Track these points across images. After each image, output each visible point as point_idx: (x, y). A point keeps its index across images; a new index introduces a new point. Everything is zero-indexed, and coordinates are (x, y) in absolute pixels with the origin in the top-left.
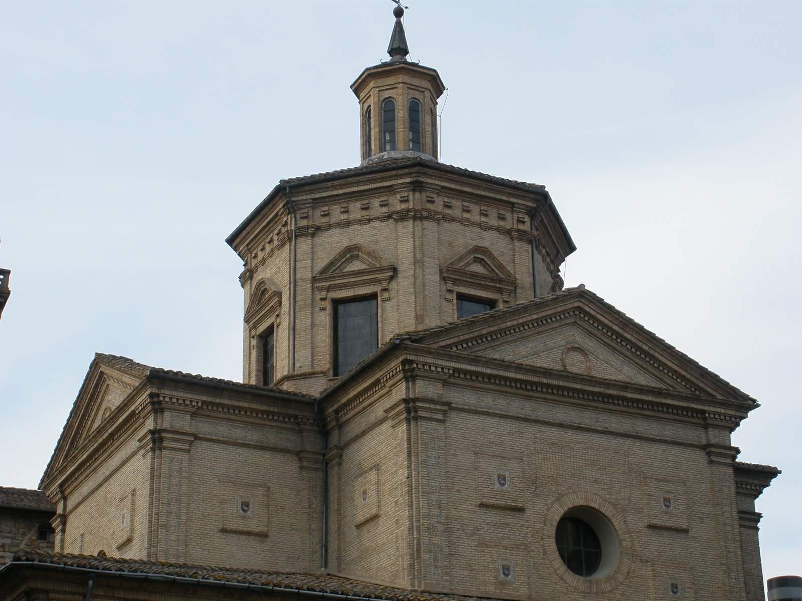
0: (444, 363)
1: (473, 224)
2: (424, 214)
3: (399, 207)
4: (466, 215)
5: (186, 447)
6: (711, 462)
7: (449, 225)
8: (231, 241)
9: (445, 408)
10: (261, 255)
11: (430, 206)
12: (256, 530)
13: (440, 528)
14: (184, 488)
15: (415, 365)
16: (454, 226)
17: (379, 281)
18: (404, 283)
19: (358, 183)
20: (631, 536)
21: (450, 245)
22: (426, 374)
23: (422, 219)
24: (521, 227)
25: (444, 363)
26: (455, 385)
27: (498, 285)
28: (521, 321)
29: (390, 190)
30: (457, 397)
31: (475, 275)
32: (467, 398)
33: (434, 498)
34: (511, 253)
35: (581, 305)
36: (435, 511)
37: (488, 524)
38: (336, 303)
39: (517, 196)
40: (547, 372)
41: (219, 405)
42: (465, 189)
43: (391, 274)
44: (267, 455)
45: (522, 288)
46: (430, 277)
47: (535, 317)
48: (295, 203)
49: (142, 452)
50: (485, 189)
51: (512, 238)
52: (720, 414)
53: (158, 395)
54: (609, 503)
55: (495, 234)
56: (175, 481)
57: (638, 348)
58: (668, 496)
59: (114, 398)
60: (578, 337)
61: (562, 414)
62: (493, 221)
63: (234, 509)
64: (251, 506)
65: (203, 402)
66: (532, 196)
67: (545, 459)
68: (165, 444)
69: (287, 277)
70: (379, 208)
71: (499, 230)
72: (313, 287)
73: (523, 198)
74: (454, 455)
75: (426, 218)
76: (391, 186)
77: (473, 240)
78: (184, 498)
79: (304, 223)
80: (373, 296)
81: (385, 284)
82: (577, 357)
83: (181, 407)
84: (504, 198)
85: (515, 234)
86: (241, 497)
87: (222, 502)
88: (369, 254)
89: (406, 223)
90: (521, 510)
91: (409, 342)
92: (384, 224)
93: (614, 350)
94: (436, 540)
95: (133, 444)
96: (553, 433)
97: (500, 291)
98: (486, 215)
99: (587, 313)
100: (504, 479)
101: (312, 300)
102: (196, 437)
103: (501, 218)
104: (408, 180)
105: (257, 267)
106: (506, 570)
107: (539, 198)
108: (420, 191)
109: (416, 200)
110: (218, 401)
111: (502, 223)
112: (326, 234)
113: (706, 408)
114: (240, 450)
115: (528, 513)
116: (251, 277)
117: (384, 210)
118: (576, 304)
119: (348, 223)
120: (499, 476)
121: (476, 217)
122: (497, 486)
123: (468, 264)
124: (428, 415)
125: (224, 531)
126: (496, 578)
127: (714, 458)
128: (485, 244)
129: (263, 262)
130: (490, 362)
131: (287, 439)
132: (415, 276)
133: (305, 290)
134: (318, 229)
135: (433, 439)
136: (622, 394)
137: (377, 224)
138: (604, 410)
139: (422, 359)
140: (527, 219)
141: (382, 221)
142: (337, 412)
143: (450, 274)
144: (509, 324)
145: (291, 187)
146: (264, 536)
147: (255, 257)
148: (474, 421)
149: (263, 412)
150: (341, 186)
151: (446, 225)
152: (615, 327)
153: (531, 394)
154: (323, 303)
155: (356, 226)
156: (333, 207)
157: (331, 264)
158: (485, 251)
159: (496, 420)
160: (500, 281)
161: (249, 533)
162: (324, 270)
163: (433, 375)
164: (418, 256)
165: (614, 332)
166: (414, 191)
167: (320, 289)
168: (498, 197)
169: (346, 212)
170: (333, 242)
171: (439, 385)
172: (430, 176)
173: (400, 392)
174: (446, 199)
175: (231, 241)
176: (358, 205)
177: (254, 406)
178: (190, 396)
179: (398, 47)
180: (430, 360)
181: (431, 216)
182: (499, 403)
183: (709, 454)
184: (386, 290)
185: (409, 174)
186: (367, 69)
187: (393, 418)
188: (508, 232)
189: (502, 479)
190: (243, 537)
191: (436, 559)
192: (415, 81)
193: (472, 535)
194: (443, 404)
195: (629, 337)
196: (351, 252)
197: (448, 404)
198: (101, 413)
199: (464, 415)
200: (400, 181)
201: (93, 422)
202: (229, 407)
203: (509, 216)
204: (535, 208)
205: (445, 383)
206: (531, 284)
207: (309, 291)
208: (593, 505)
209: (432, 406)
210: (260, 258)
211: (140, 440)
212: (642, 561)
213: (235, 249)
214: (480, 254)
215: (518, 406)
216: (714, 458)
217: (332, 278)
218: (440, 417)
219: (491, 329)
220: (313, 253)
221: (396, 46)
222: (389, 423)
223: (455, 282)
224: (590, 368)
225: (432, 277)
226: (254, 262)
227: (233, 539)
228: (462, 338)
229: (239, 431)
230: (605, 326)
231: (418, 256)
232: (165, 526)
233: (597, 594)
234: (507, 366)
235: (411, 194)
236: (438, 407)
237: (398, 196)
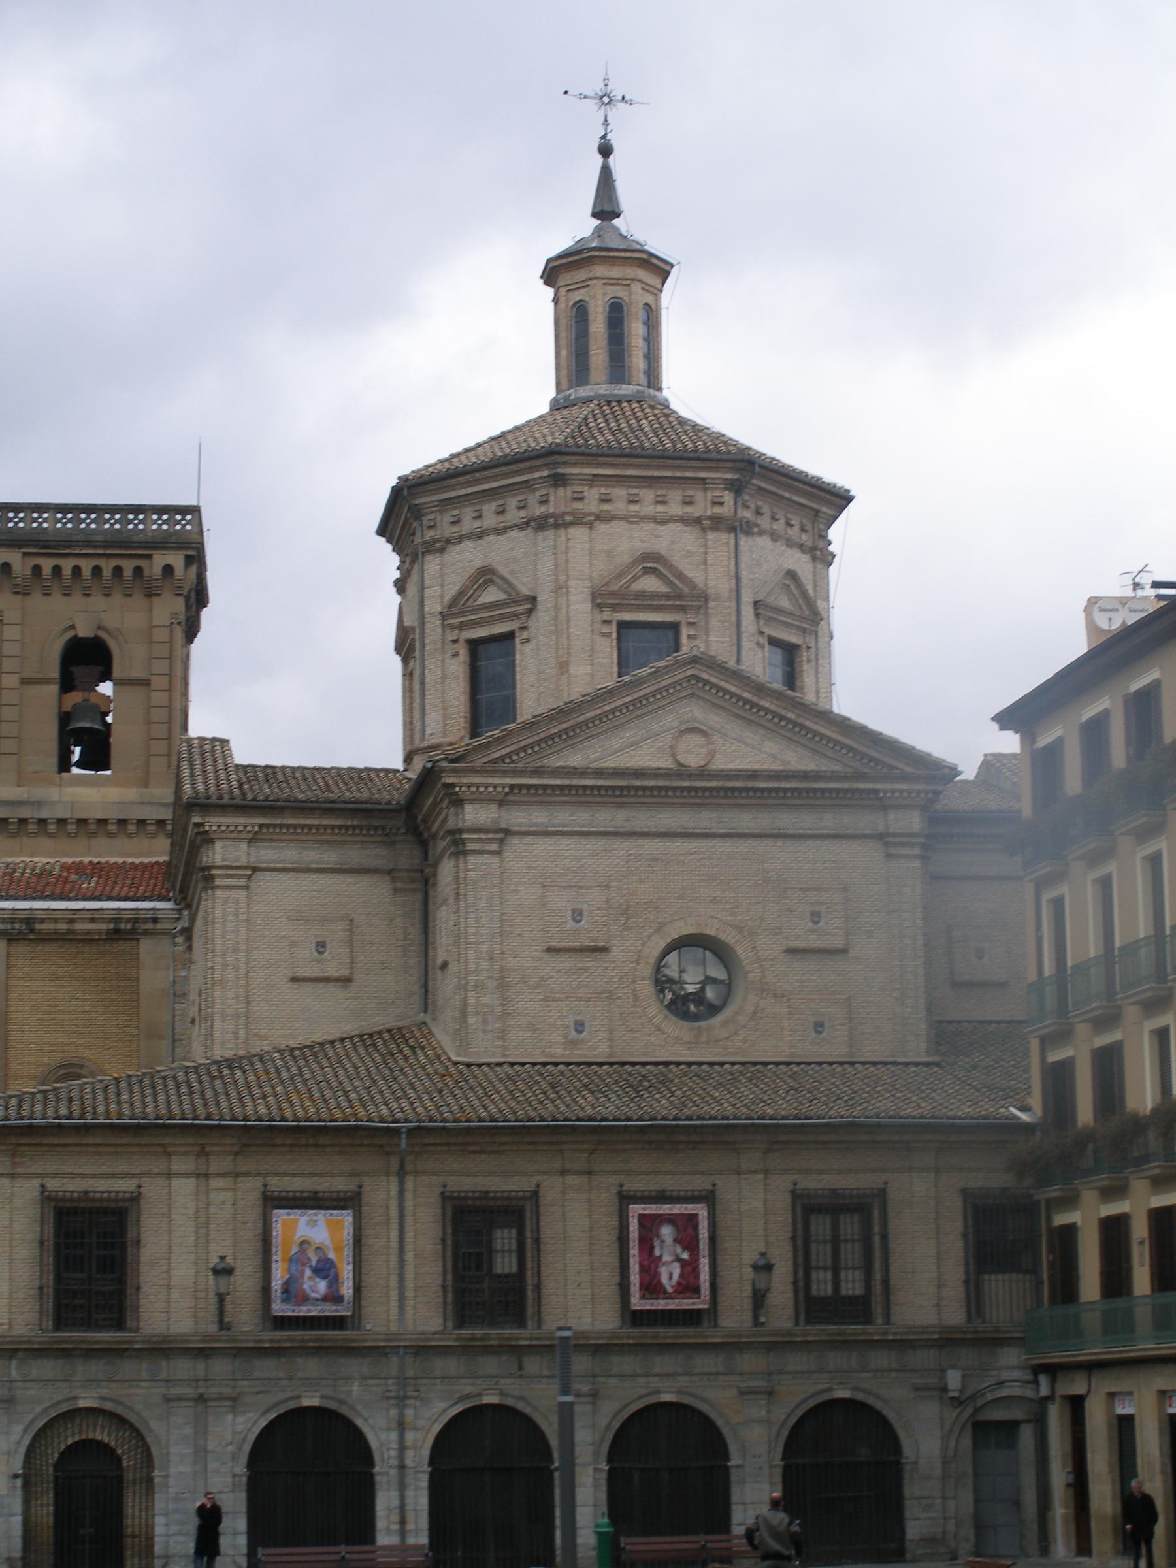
0: (496, 781)
1: (644, 519)
2: (568, 519)
3: (539, 511)
5: (242, 883)
6: (888, 856)
7: (608, 526)
8: (382, 531)
9: (501, 835)
11: (578, 505)
12: (336, 974)
13: (492, 984)
15: (457, 789)
16: (617, 527)
17: (516, 616)
19: (488, 479)
20: (761, 966)
21: (609, 554)
22: (473, 797)
23: (566, 525)
24: (717, 510)
25: (496, 781)
27: (678, 603)
28: (607, 708)
29: (527, 486)
30: (517, 817)
31: (641, 595)
32: (538, 817)
33: (484, 948)
34: (702, 550)
35: (696, 672)
36: (485, 965)
37: (559, 971)
38: (474, 646)
39: (709, 469)
40: (638, 773)
41: (281, 826)
42: (628, 472)
43: (529, 606)
44: (349, 879)
45: (717, 599)
46: (578, 607)
47: (628, 699)
50: (658, 468)
51: (704, 530)
52: (901, 791)
53: (202, 824)
54: (731, 926)
55: (679, 527)
56: (230, 926)
57: (782, 718)
58: (817, 908)
60: (695, 711)
61: (668, 819)
62: (676, 509)
63: (306, 952)
64: (328, 946)
65: (261, 826)
66: (730, 465)
67: (641, 881)
68: (218, 882)
70: (515, 511)
71: (684, 520)
72: (443, 626)
73: (717, 469)
74: (514, 891)
75: (571, 524)
76: (527, 481)
77: (643, 541)
78: (243, 946)
79: (429, 534)
80: (511, 636)
81: (523, 619)
82: (695, 740)
83: (233, 835)
84: (688, 474)
86: (316, 936)
87: (293, 944)
88: (503, 578)
89: (547, 533)
90: (604, 950)
91: (444, 764)
92: (522, 534)
93: (750, 722)
94: (486, 1000)
96: (653, 846)
97: (683, 609)
98: (664, 503)
100: (581, 914)
101: (443, 642)
103: (688, 502)
104: (546, 473)
106: (579, 1026)
108: (564, 485)
109: (559, 501)
110: (278, 821)
111: (688, 509)
112: (457, 548)
113: (879, 786)
114: (314, 877)
115: (615, 952)
117: (523, 513)
118: (689, 673)
119: (480, 535)
120: (574, 911)
121: (648, 508)
122: (571, 924)
123: (635, 578)
124: (477, 847)
125: (294, 979)
126: (565, 1037)
127: (893, 851)
130: (556, 772)
131: (374, 855)
133: (433, 625)
134: (448, 541)
136: (750, 784)
137: (514, 534)
138: (730, 806)
139: (465, 780)
140: (728, 497)
141: (521, 529)
144: (589, 715)
145: (409, 487)
146: (347, 980)
149: (340, 827)
150: (468, 484)
151: (603, 527)
152: (746, 695)
153: (623, 800)
154: (456, 646)
155: (491, 538)
156: (465, 510)
157: (461, 593)
158: (657, 557)
159: (575, 839)
160: (679, 597)
161: (326, 980)
162: (452, 605)
163: (482, 797)
164: (562, 578)
165: (746, 701)
166: (555, 486)
167: (453, 627)
168: (678, 474)
169: (479, 517)
170: (465, 558)
171: (494, 807)
172: (575, 464)
174: (603, 490)
175: (382, 531)
176: (493, 506)
177: (326, 822)
178: (242, 820)
179: (606, 208)
180: (477, 780)
181: (579, 520)
182: (580, 818)
183: (887, 844)
184: (524, 628)
185: (546, 466)
186: (549, 261)
188: (698, 521)
189: (577, 915)
190: (321, 985)
191: (485, 1022)
192: (615, 272)
193: (536, 988)
194: (497, 831)
195: (767, 705)
196: (485, 576)
197: (507, 832)
199: (528, 839)
200: (537, 475)
202: (295, 827)
203: (699, 496)
204: (737, 480)
205: (501, 803)
206: (731, 591)
207: (439, 629)
208: (708, 931)
209: (483, 836)
212: (775, 996)
214: (652, 563)
215: (605, 818)
216: (893, 851)
217: (462, 613)
218: (494, 847)
219: (565, 726)
220: (442, 576)
221: (597, 210)
223: (615, 608)
224: (711, 755)
225: (579, 605)
227: (308, 988)
228: (523, 744)
229: (312, 853)
232: (221, 982)
233: (707, 1043)
234: (582, 773)
235: (552, 490)
236: (490, 836)
237: (538, 494)
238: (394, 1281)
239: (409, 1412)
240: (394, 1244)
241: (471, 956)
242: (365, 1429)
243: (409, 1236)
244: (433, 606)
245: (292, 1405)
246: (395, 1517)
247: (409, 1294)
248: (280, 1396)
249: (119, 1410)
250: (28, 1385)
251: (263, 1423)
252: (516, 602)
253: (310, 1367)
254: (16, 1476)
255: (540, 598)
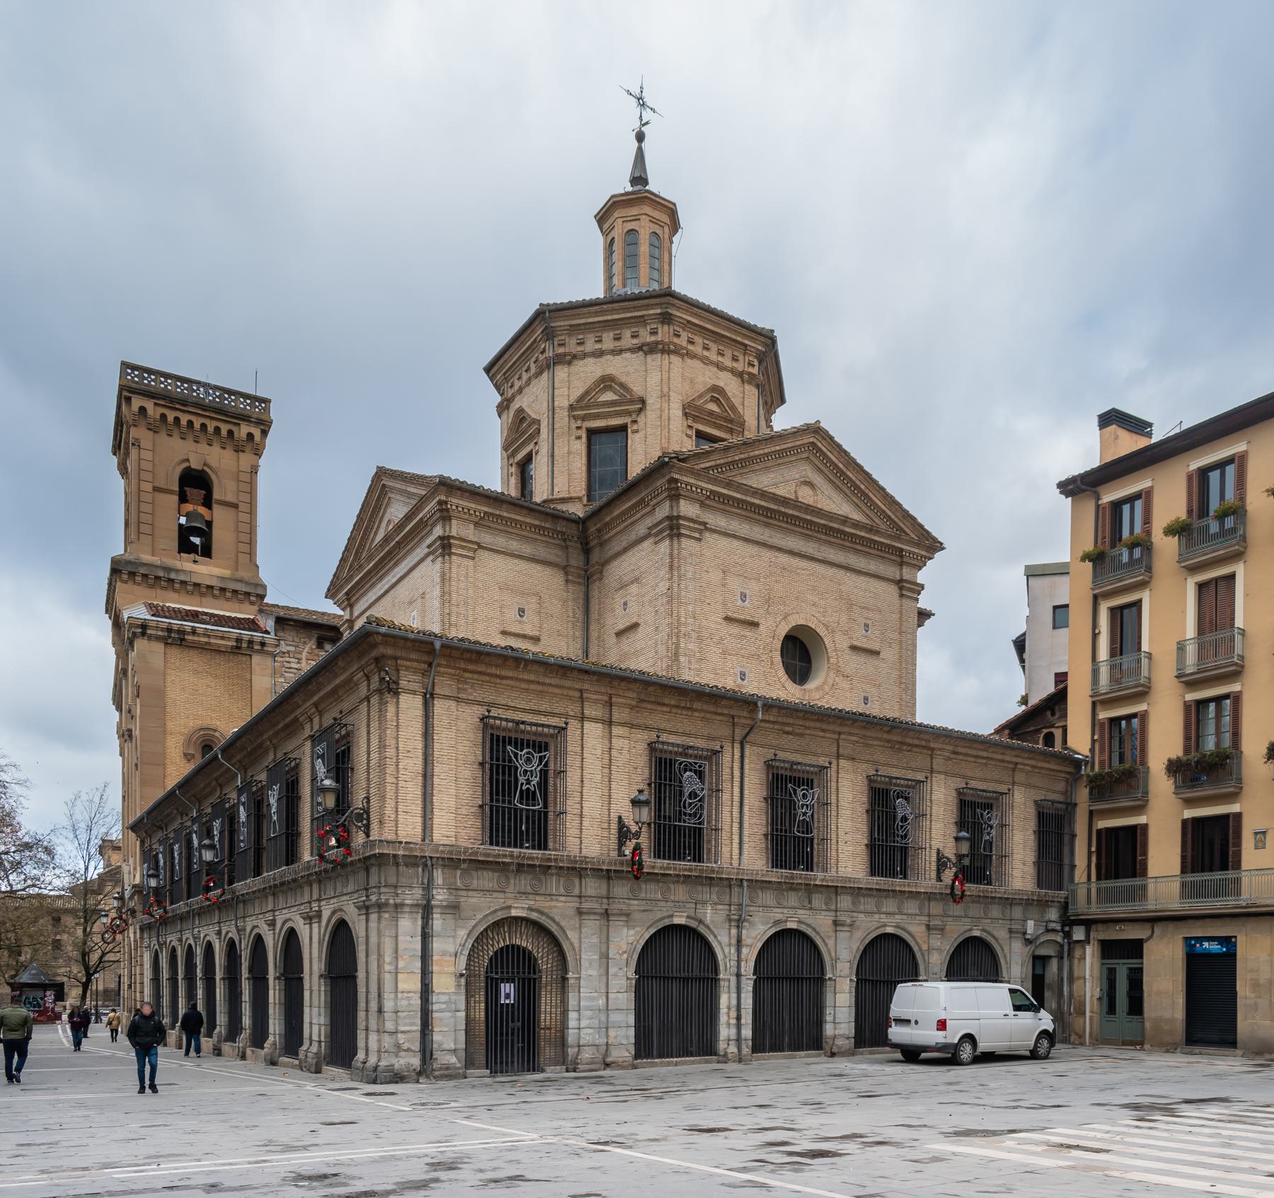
1: (712, 363)
4: (706, 353)
8: (488, 370)
10: (517, 384)
14: (470, 591)
16: (696, 363)
17: (629, 413)
18: (650, 418)
26: (709, 507)
38: (591, 433)
40: (784, 501)
44: (539, 567)
48: (547, 334)
49: (431, 557)
55: (729, 375)
59: (397, 511)
62: (728, 362)
66: (762, 339)
69: (545, 404)
71: (733, 371)
80: (624, 428)
85: (746, 376)
88: (622, 385)
95: (421, 551)
99: (819, 450)
102: (480, 546)
105: (513, 397)
107: (769, 342)
111: (735, 365)
116: (508, 407)
123: (706, 402)
128: (721, 384)
129: (520, 391)
132: (661, 409)
133: (562, 417)
135: (691, 555)
140: (756, 363)
142: (599, 531)
143: (691, 411)
147: (512, 386)
148: (724, 542)
149: (536, 526)
157: (587, 393)
159: (741, 543)
164: (665, 390)
173: (663, 511)
187: (656, 535)
197: (705, 524)
198: (384, 525)
199: (715, 536)
201: (376, 534)
203: (741, 358)
205: (702, 505)
210: (516, 388)
211: (429, 547)
213: (491, 380)
214: (717, 393)
217: (588, 407)
218: (697, 535)
222: (651, 540)
225: (677, 412)
226: (510, 393)
229: (515, 543)
230: (832, 463)
231: (665, 390)
238: (736, 826)
239: (744, 932)
240: (737, 798)
241: (683, 613)
242: (715, 944)
243: (746, 792)
244: (562, 402)
245: (667, 922)
246: (733, 1014)
247: (746, 839)
248: (659, 915)
249: (543, 920)
250: (470, 893)
251: (647, 936)
252: (632, 402)
253: (680, 892)
254: (462, 975)
255: (649, 401)
